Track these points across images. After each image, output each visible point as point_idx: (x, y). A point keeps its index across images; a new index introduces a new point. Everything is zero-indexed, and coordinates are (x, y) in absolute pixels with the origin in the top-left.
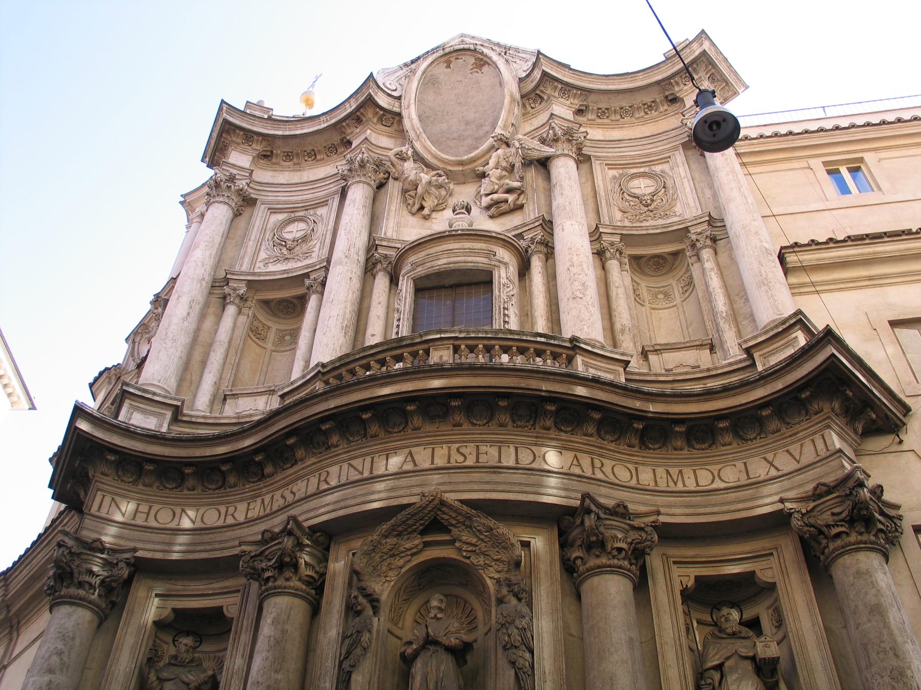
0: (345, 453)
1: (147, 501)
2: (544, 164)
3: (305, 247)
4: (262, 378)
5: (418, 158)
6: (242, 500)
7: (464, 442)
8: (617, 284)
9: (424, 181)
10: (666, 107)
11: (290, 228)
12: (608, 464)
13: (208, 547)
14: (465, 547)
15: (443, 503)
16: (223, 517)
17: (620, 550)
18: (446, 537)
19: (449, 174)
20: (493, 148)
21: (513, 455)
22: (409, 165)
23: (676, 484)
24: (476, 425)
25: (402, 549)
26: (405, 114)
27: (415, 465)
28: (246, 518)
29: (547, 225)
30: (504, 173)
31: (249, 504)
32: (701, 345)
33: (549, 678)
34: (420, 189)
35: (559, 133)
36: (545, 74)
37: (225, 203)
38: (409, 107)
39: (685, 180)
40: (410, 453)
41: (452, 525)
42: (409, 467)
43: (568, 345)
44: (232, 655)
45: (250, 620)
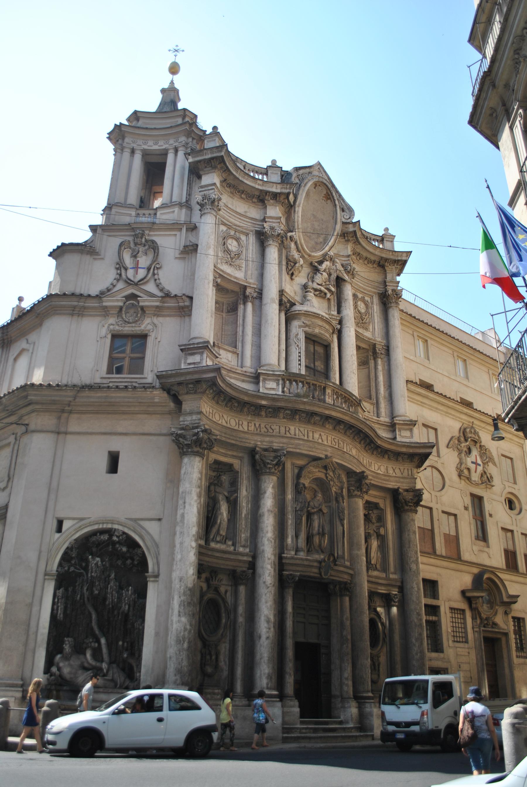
1: (212, 407)
2: (339, 281)
3: (238, 262)
5: (296, 243)
6: (245, 419)
11: (230, 241)
16: (237, 425)
18: (325, 472)
22: (293, 245)
26: (297, 209)
27: (322, 441)
29: (340, 322)
31: (248, 423)
34: (297, 265)
38: (299, 206)
40: (320, 435)
42: (320, 441)
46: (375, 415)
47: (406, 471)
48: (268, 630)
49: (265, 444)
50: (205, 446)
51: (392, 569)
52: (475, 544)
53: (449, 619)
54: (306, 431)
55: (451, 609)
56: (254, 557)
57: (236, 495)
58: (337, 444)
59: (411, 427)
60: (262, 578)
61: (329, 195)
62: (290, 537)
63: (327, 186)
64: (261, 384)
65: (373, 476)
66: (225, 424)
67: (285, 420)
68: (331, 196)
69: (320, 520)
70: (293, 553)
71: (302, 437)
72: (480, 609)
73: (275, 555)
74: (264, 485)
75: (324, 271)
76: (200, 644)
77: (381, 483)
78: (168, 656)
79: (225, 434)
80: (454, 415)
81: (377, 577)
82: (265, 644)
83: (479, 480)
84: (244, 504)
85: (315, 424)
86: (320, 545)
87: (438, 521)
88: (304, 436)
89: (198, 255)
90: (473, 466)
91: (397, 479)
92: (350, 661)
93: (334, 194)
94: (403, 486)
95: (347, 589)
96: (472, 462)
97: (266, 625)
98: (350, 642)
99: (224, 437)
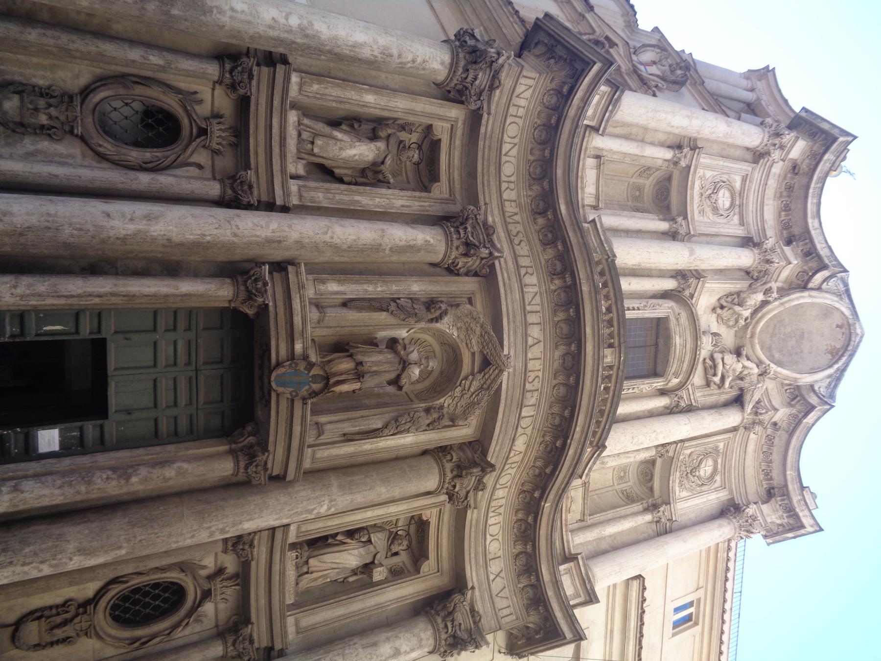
1: (526, 114)
2: (738, 401)
3: (708, 210)
4: (609, 177)
5: (765, 303)
6: (519, 195)
7: (543, 380)
8: (637, 456)
9: (744, 312)
10: (765, 486)
11: (727, 194)
12: (512, 472)
14: (468, 383)
15: (501, 371)
17: (454, 486)
18: (476, 370)
19: (746, 327)
20: (759, 363)
21: (529, 415)
22: (760, 297)
24: (554, 388)
25: (472, 336)
26: (806, 294)
28: (505, 200)
29: (690, 409)
30: (737, 373)
31: (515, 201)
32: (584, 515)
33: (374, 446)
34: (737, 308)
35: (761, 417)
36: (813, 408)
37: (761, 143)
38: (810, 296)
39: (705, 500)
40: (540, 341)
41: (485, 375)
42: (530, 341)
44: (403, 196)
45: (428, 208)
48: (129, 217)
54: (538, 308)
61: (837, 354)
63: (848, 345)
65: (477, 521)
66: (506, 147)
67: (543, 262)
68: (837, 357)
70: (310, 293)
73: (299, 244)
75: (744, 367)
77: (470, 547)
79: (490, 147)
81: (283, 573)
84: (377, 200)
85: (556, 324)
89: (699, 136)
91: (485, 586)
93: (844, 359)
94: (478, 597)
99: (484, 145)
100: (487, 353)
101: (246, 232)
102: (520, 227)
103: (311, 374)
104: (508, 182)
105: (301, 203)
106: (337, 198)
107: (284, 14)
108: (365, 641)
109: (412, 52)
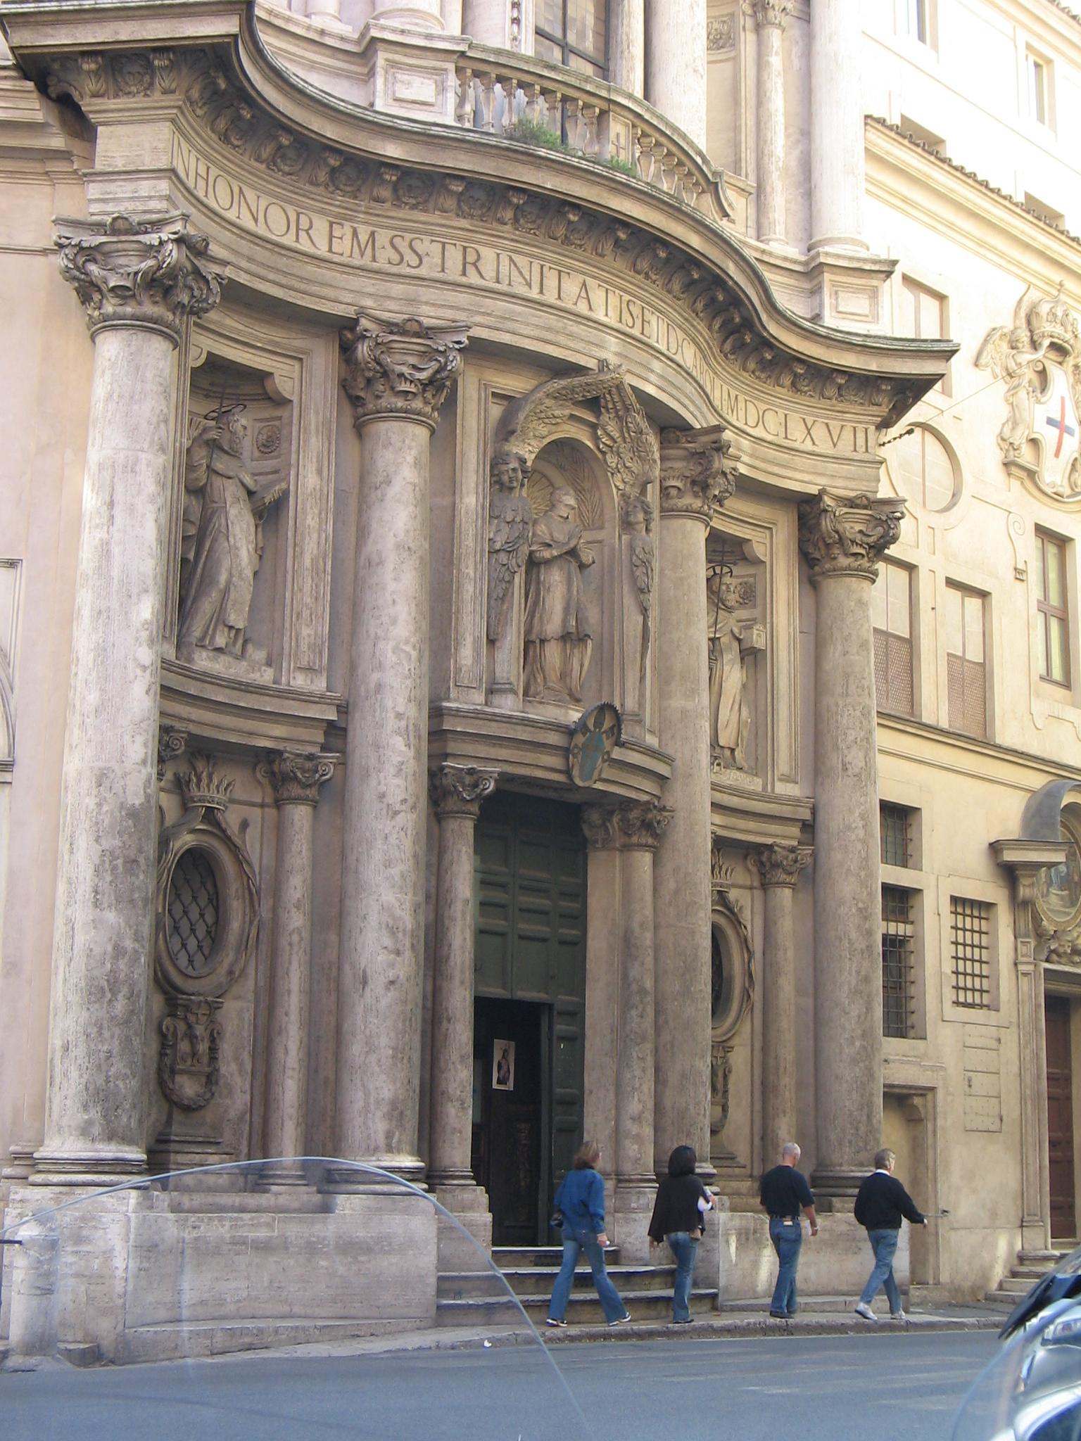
0: (512, 240)
1: (207, 157)
6: (321, 212)
13: (284, 281)
23: (732, 411)
27: (590, 309)
31: (331, 224)
32: (743, 190)
40: (584, 284)
42: (582, 308)
43: (710, 176)
45: (321, 419)
46: (752, 232)
47: (847, 435)
49: (392, 305)
50: (184, 298)
51: (783, 766)
52: (1038, 696)
53: (948, 935)
55: (955, 900)
56: (344, 709)
57: (284, 485)
58: (638, 322)
59: (875, 283)
60: (373, 782)
62: (469, 641)
64: (380, 81)
66: (247, 222)
67: (464, 223)
69: (569, 590)
70: (478, 698)
71: (521, 290)
72: (1042, 906)
74: (384, 458)
76: (158, 1002)
78: (58, 1043)
80: (1002, 255)
82: (384, 1002)
83: (1065, 482)
84: (309, 521)
86: (564, 675)
87: (932, 613)
88: (530, 285)
90: (1049, 436)
92: (650, 1061)
95: (648, 826)
96: (1050, 422)
97: (387, 941)
98: (650, 999)
99: (247, 272)
100: (583, 396)
101: (410, 789)
102: (383, 237)
103: (592, 729)
104: (298, 229)
105: (325, 675)
106: (309, 600)
107: (139, 672)
108: (839, 690)
109: (158, 423)
